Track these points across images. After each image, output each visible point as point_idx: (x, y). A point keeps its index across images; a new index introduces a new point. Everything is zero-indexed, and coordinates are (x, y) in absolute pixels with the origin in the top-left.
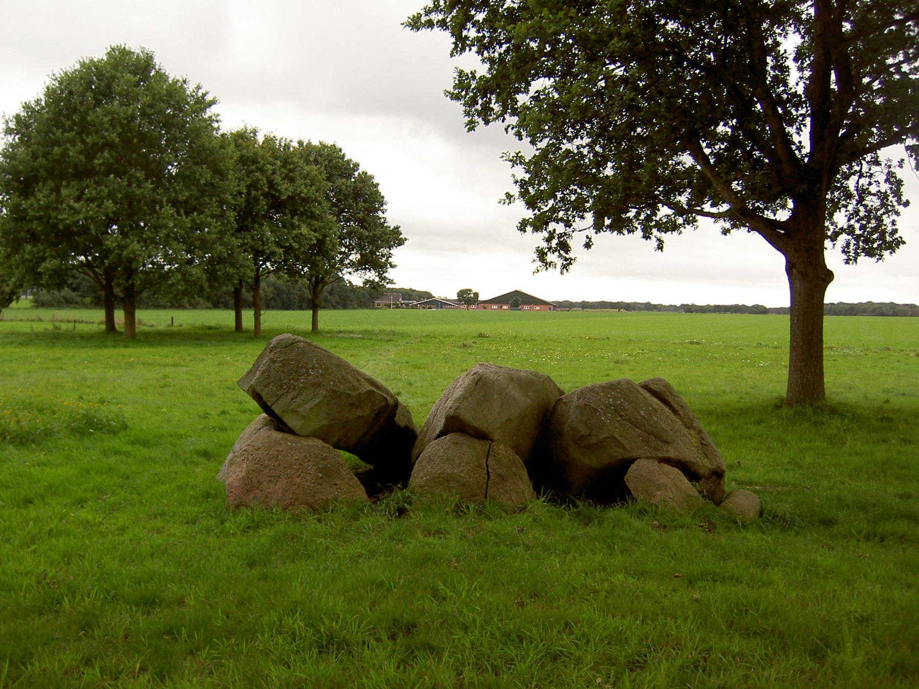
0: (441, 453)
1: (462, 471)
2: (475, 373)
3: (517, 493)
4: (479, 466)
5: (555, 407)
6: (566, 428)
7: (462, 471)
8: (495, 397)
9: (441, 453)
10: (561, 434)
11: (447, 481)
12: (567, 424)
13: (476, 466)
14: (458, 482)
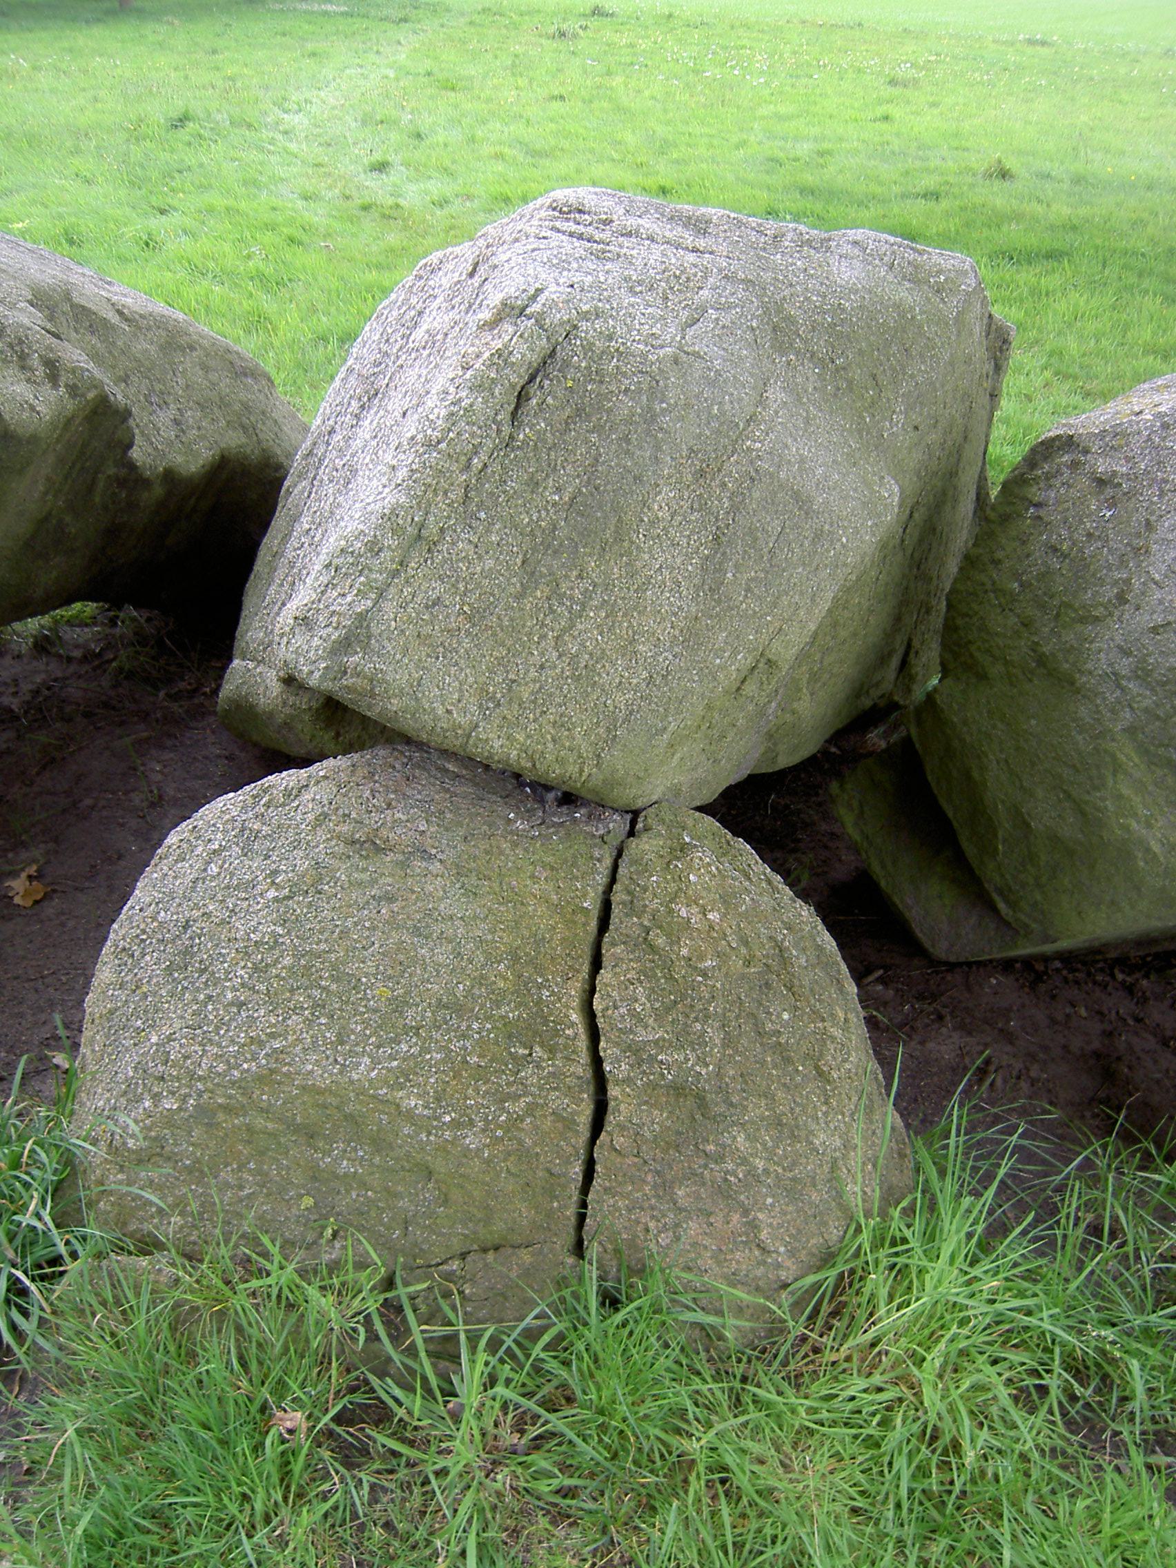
0: (258, 922)
1: (402, 1078)
2: (511, 311)
3: (792, 1190)
4: (537, 1030)
5: (1017, 483)
6: (1104, 650)
7: (402, 1078)
8: (663, 501)
9: (258, 922)
10: (1057, 676)
11: (311, 1134)
12: (1114, 633)
13: (511, 1032)
14: (379, 1144)
